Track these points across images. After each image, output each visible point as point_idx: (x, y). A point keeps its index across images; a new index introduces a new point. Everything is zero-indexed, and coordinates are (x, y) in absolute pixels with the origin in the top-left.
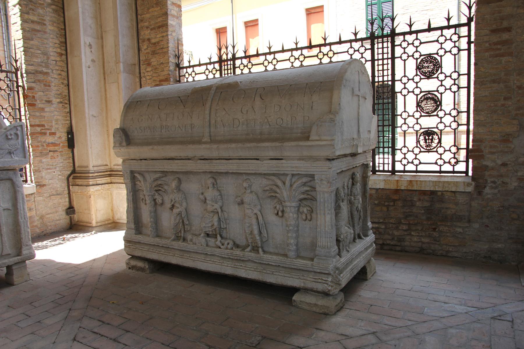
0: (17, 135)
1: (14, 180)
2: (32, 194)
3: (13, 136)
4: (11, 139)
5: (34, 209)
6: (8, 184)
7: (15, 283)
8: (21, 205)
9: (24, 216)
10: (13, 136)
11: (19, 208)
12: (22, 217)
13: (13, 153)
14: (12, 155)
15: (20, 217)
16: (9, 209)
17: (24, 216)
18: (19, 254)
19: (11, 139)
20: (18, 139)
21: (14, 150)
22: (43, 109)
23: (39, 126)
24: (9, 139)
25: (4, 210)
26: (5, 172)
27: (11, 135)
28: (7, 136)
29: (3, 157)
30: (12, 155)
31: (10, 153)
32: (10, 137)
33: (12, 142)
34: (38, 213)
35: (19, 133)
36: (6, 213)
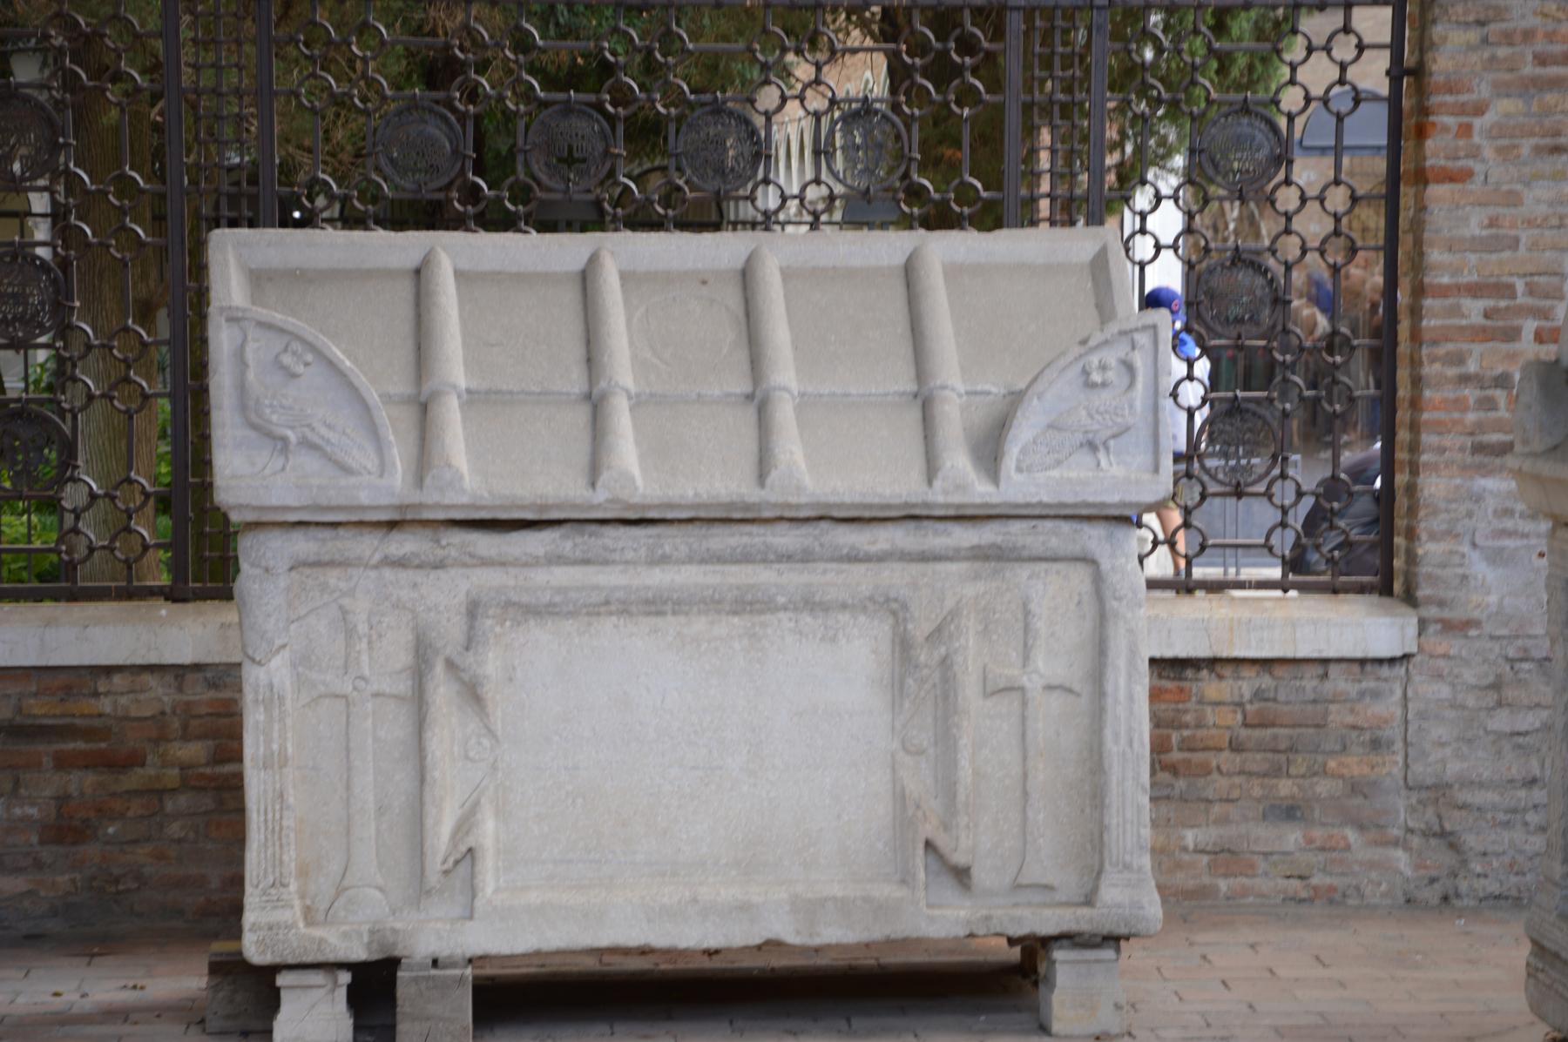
0: (1129, 367)
1: (1105, 565)
2: (1392, 661)
3: (1111, 375)
4: (1104, 385)
5: (1399, 745)
6: (1079, 577)
7: (1056, 1027)
8: (1122, 681)
9: (1130, 730)
10: (1111, 375)
11: (1109, 688)
12: (1117, 735)
13: (1107, 449)
14: (1102, 455)
15: (1108, 733)
16: (1070, 691)
17: (1130, 730)
18: (1089, 901)
19: (1104, 385)
20: (1132, 384)
21: (1109, 433)
22: (1513, 199)
23: (1475, 290)
24: (1093, 386)
25: (1049, 688)
26: (1066, 527)
27: (1103, 368)
28: (1086, 372)
29: (1059, 463)
30: (1102, 455)
31: (1092, 446)
32: (1096, 377)
33: (1103, 398)
34: (1417, 768)
35: (1140, 361)
36: (1056, 701)
